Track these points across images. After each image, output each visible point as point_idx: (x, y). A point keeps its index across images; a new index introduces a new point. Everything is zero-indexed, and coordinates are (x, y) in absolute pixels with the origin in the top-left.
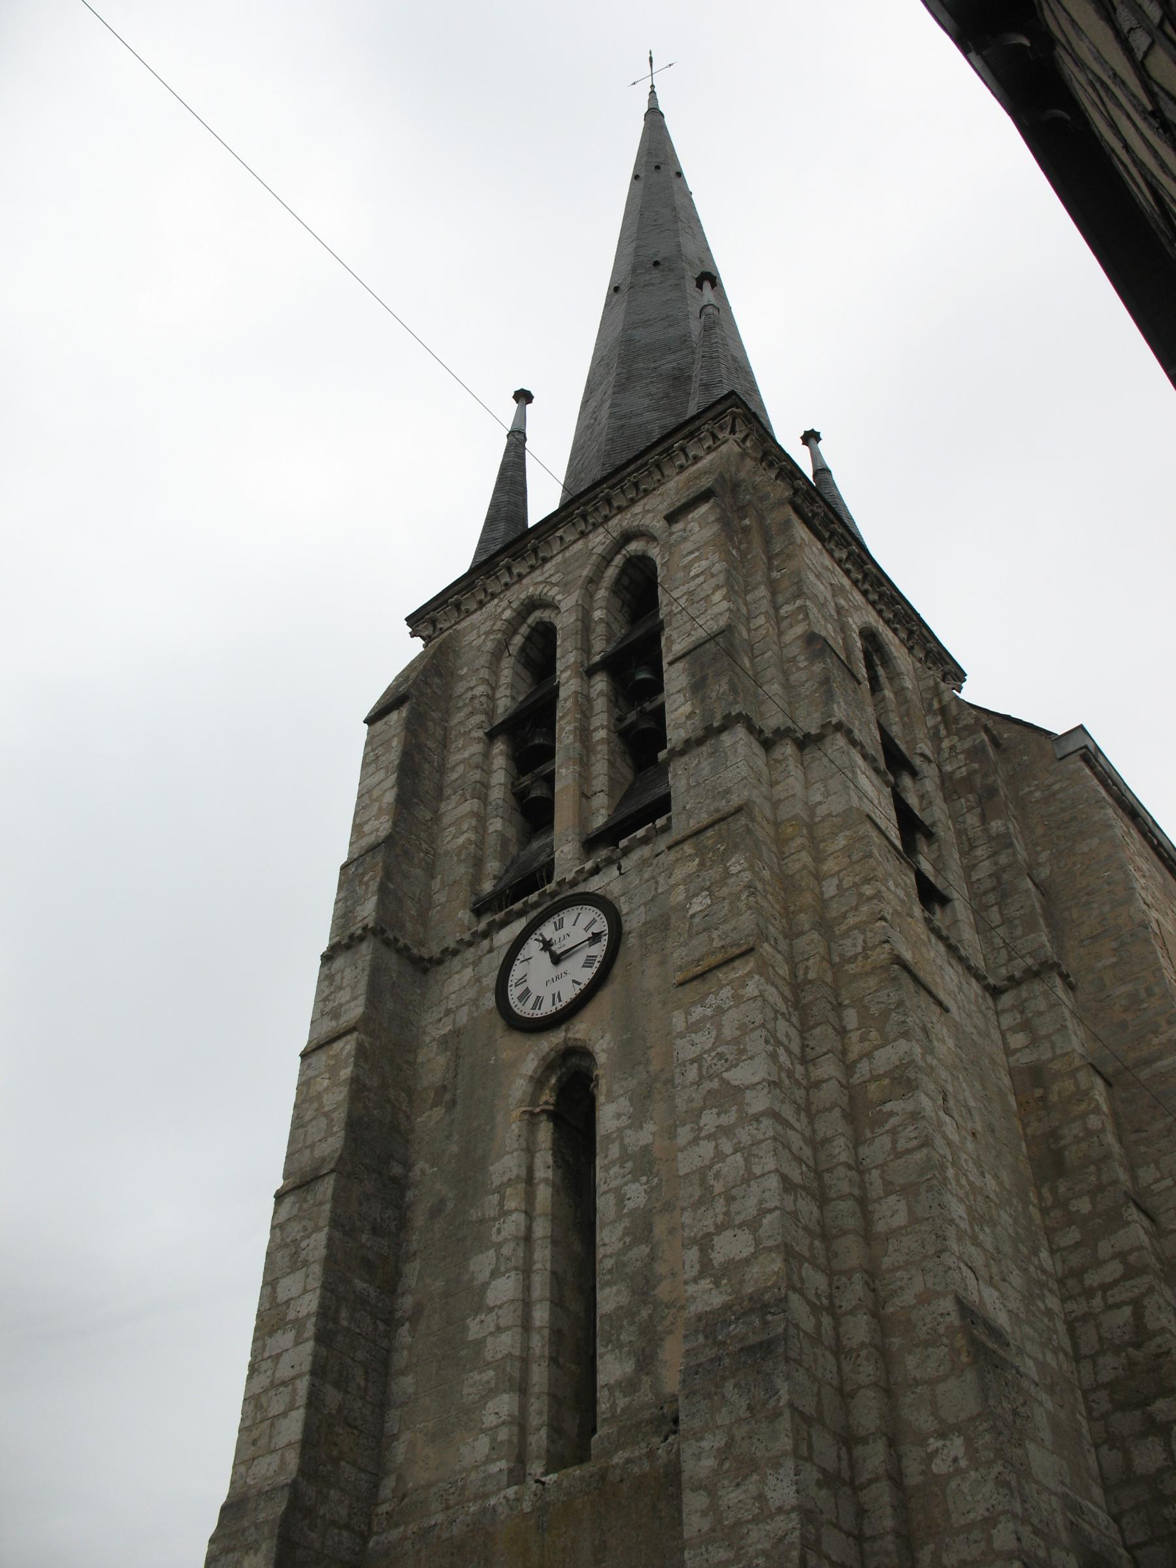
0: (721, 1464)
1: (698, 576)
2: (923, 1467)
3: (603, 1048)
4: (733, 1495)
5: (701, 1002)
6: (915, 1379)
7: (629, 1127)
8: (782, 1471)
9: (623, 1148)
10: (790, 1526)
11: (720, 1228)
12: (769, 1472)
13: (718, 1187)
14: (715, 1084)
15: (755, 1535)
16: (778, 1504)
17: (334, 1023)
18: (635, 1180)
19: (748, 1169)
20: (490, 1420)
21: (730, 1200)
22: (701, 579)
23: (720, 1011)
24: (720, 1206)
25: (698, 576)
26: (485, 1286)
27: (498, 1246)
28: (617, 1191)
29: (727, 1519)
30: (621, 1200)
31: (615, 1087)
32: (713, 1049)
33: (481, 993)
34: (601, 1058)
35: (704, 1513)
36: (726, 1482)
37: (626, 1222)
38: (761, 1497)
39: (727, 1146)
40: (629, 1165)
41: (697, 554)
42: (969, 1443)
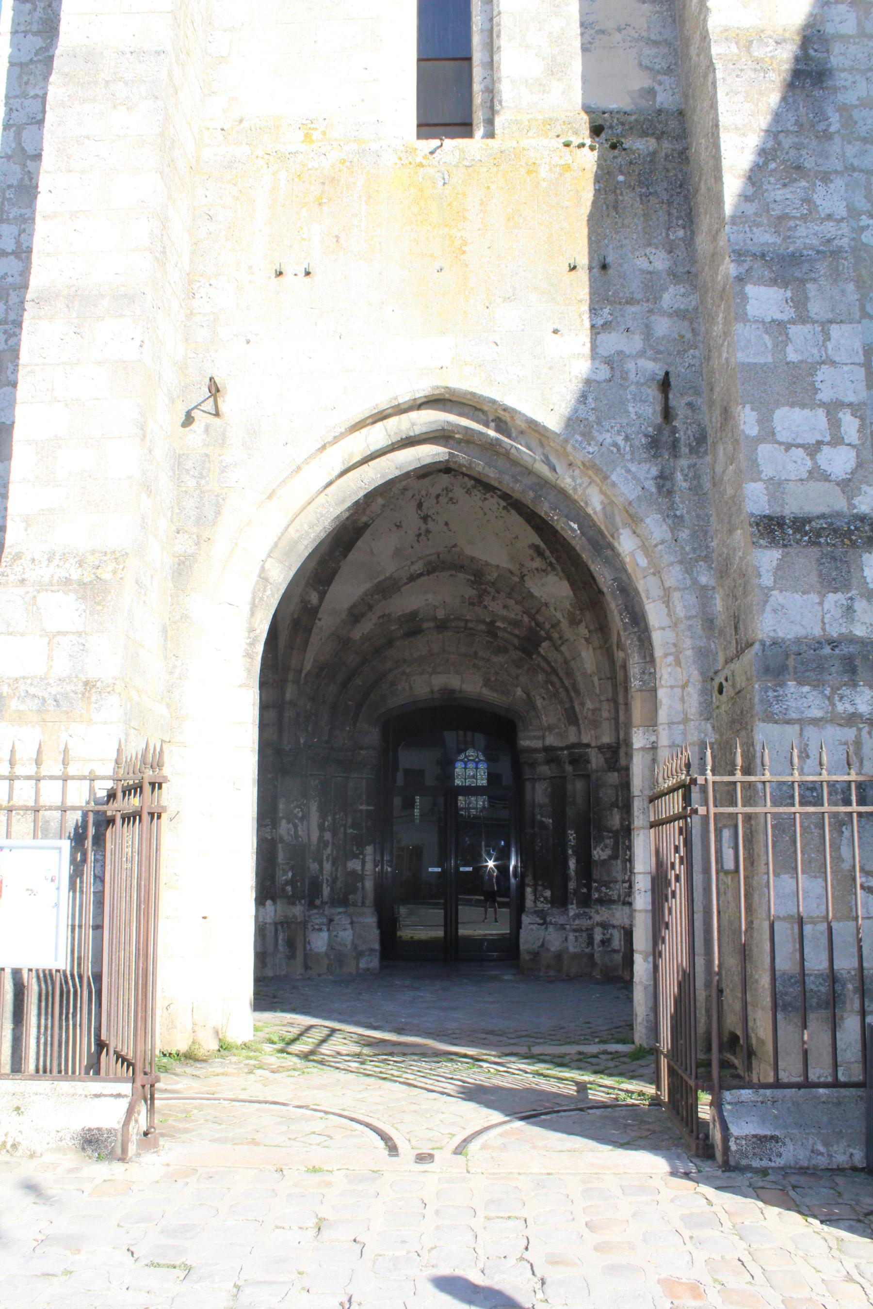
0: (766, 163)
2: (854, 235)
4: (780, 192)
6: (852, 165)
8: (832, 186)
10: (840, 232)
12: (818, 183)
15: (802, 231)
16: (827, 211)
29: (774, 210)
36: (772, 180)
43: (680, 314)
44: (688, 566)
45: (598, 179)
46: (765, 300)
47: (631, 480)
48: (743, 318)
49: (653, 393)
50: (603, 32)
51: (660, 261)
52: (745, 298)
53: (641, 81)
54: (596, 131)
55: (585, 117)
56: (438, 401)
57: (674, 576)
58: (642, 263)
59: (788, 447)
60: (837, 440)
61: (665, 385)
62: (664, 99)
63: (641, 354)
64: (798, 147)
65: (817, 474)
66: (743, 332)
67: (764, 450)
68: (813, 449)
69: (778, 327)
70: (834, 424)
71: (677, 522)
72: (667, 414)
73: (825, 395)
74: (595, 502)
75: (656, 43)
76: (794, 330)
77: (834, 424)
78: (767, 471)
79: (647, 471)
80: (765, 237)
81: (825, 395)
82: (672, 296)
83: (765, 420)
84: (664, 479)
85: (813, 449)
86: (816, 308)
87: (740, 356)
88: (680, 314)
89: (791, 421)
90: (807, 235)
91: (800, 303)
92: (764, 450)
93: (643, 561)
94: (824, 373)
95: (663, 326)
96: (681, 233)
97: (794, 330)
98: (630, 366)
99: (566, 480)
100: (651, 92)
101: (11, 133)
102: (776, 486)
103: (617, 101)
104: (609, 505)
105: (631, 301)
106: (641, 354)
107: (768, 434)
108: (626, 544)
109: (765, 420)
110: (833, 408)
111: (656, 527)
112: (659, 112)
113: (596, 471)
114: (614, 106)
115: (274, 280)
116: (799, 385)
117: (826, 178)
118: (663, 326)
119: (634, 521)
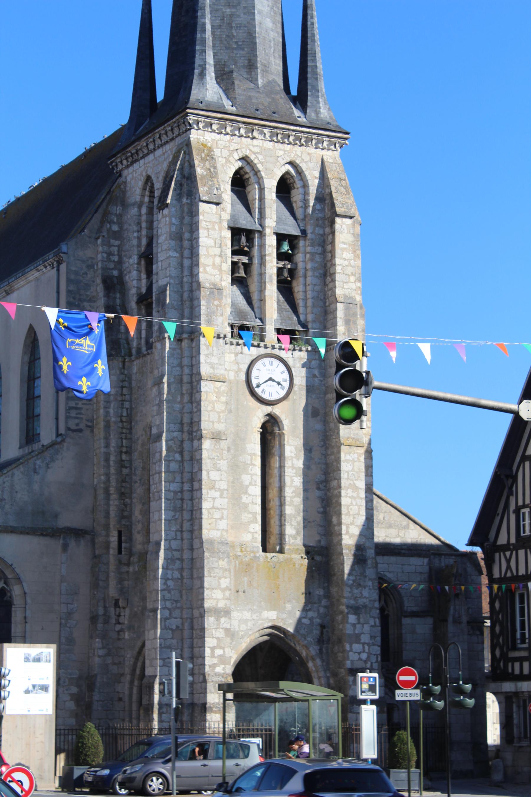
1: (345, 259)
3: (286, 423)
5: (349, 453)
7: (295, 458)
9: (293, 464)
11: (352, 524)
13: (351, 513)
14: (352, 483)
15: (359, 601)
17: (212, 371)
18: (296, 476)
19: (359, 511)
20: (252, 530)
21: (354, 518)
22: (346, 263)
23: (354, 461)
24: (351, 518)
25: (345, 259)
26: (247, 487)
27: (252, 475)
28: (291, 477)
30: (292, 481)
31: (290, 441)
32: (351, 471)
33: (239, 370)
34: (286, 427)
35: (350, 592)
37: (294, 489)
38: (361, 593)
39: (354, 503)
40: (294, 471)
41: (345, 246)
42: (373, 583)
43: (325, 607)
44: (325, 671)
45: (308, 569)
46: (352, 618)
47: (313, 650)
48: (347, 622)
49: (319, 627)
50: (309, 522)
51: (321, 592)
52: (348, 618)
53: (318, 538)
54: (307, 553)
55: (304, 549)
56: (272, 627)
57: (322, 674)
58: (317, 592)
59: (355, 653)
60: (364, 651)
61: (323, 626)
62: (323, 543)
63: (317, 617)
64: (360, 579)
65: (360, 659)
66: (348, 626)
67: (351, 653)
68: (359, 653)
69: (354, 625)
70: (364, 647)
71: (323, 661)
72: (322, 633)
73: (362, 641)
74: (304, 654)
75: (321, 526)
76: (358, 626)
77: (364, 647)
78: (351, 658)
79: (317, 648)
80: (352, 602)
81: (362, 641)
82: (324, 602)
83: (351, 647)
84: (321, 650)
85: (359, 653)
86: (362, 620)
87: (347, 632)
88: (325, 607)
89: (357, 647)
90: (361, 601)
91: (358, 619)
92: (351, 654)
93: (314, 669)
94: (362, 636)
95: (322, 610)
96: (326, 585)
97: (358, 626)
98: (314, 620)
99: (298, 648)
100: (320, 541)
101: (168, 542)
102: (352, 662)
103: (312, 544)
104: (307, 654)
105: (315, 603)
106: (317, 617)
107: (351, 650)
108: (310, 664)
109: (351, 647)
110: (364, 644)
111: (319, 662)
112: (322, 547)
113: (307, 647)
114: (311, 545)
115: (236, 594)
116: (357, 638)
117: (365, 587)
118: (322, 610)
119: (313, 659)
